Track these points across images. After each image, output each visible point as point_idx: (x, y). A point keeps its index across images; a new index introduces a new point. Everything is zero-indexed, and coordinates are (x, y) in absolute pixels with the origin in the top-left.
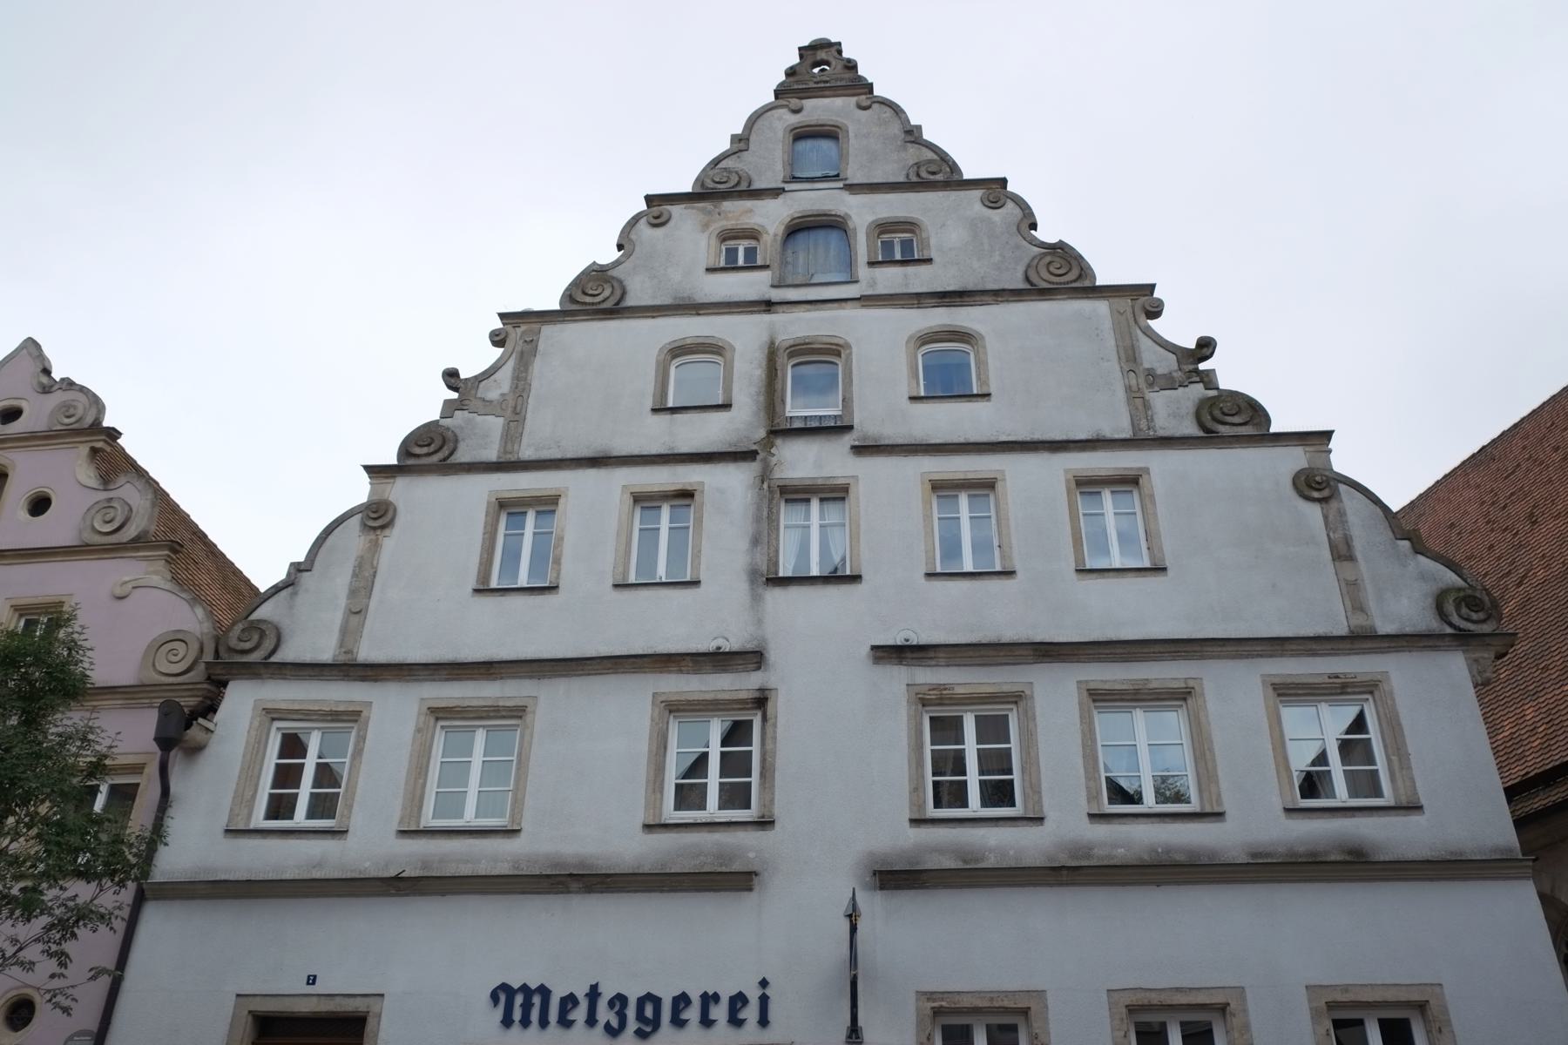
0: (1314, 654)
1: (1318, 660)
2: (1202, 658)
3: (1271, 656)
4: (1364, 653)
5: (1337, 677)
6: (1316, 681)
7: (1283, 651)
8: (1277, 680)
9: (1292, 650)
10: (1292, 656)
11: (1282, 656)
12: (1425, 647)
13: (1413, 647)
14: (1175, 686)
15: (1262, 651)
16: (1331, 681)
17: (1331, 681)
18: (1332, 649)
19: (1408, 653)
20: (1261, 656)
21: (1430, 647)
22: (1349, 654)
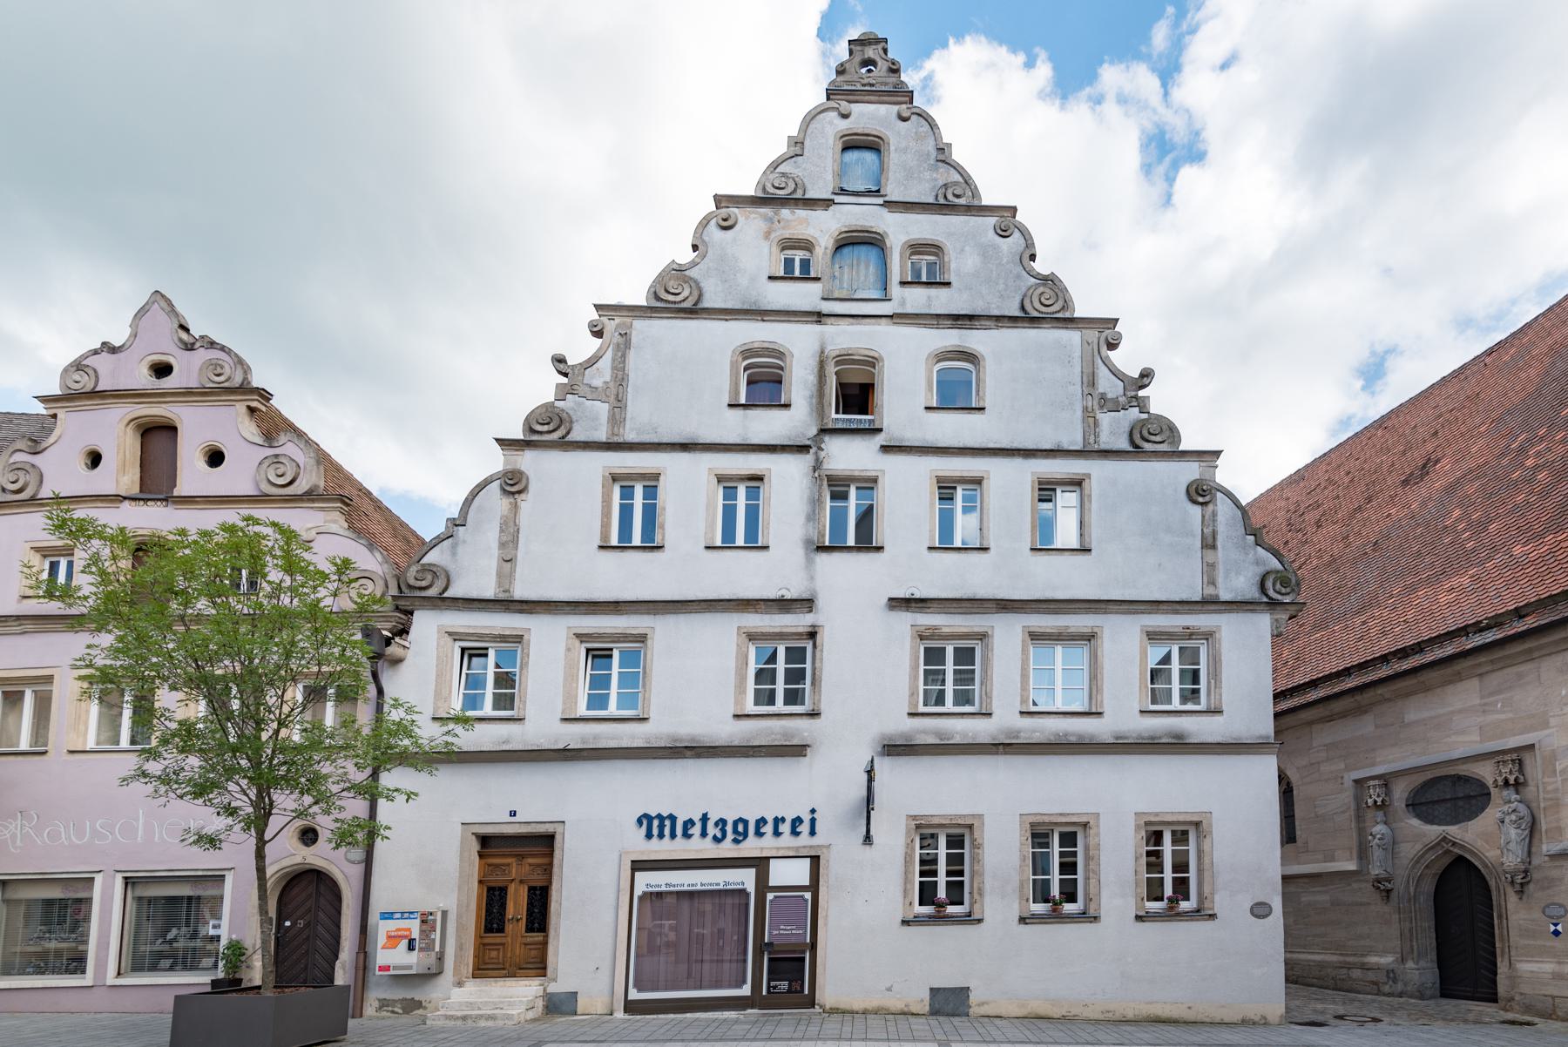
0: (1176, 612)
2: (1105, 613)
3: (1150, 613)
10: (1162, 613)
11: (1156, 613)
19: (1235, 614)
20: (1143, 613)
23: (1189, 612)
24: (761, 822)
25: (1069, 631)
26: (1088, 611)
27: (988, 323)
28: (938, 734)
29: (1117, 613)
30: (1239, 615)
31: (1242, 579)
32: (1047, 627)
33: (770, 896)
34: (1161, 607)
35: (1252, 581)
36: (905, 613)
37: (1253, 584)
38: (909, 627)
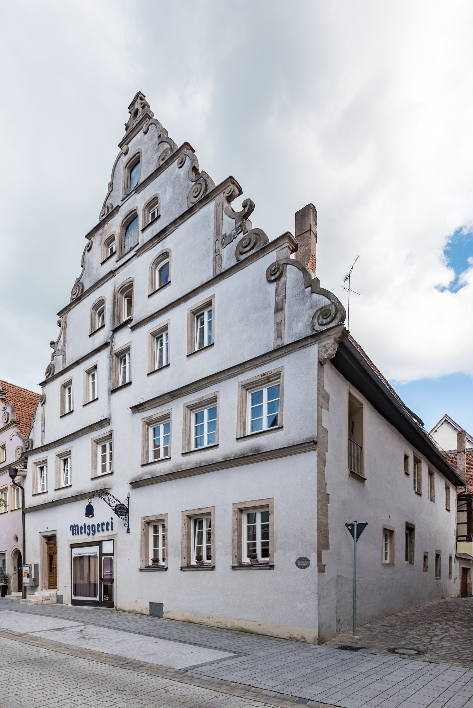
0: (257, 366)
1: (259, 368)
2: (220, 382)
3: (243, 373)
4: (276, 359)
5: (265, 375)
6: (257, 379)
7: (246, 369)
8: (243, 384)
9: (249, 368)
10: (250, 370)
11: (246, 371)
12: (300, 347)
13: (296, 349)
14: (211, 397)
15: (238, 372)
16: (262, 377)
17: (262, 377)
18: (263, 362)
20: (239, 374)
21: (303, 346)
22: (270, 362)
23: (264, 363)
24: (98, 525)
25: (204, 399)
26: (211, 384)
27: (172, 228)
28: (151, 473)
29: (225, 379)
30: (297, 352)
31: (300, 324)
32: (194, 400)
33: (103, 558)
34: (247, 366)
35: (307, 323)
36: (138, 414)
37: (308, 325)
38: (141, 420)
